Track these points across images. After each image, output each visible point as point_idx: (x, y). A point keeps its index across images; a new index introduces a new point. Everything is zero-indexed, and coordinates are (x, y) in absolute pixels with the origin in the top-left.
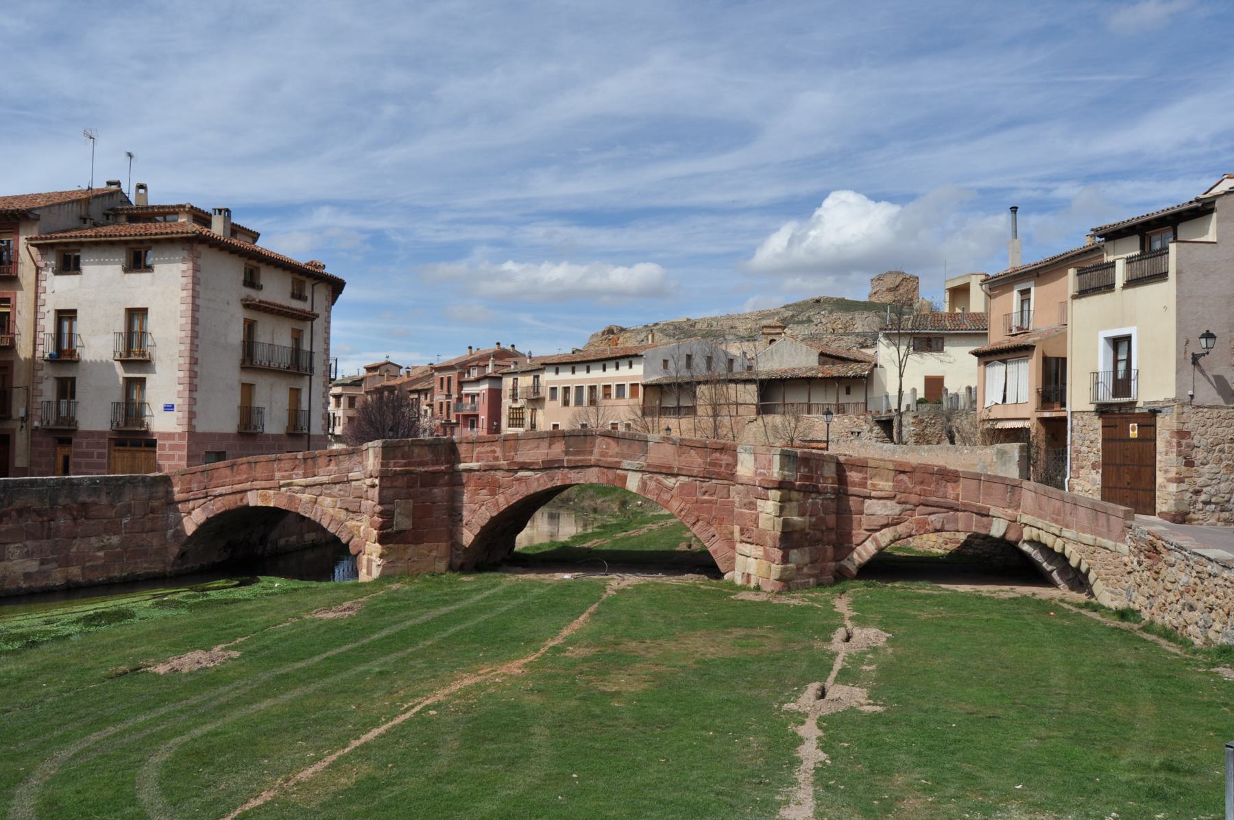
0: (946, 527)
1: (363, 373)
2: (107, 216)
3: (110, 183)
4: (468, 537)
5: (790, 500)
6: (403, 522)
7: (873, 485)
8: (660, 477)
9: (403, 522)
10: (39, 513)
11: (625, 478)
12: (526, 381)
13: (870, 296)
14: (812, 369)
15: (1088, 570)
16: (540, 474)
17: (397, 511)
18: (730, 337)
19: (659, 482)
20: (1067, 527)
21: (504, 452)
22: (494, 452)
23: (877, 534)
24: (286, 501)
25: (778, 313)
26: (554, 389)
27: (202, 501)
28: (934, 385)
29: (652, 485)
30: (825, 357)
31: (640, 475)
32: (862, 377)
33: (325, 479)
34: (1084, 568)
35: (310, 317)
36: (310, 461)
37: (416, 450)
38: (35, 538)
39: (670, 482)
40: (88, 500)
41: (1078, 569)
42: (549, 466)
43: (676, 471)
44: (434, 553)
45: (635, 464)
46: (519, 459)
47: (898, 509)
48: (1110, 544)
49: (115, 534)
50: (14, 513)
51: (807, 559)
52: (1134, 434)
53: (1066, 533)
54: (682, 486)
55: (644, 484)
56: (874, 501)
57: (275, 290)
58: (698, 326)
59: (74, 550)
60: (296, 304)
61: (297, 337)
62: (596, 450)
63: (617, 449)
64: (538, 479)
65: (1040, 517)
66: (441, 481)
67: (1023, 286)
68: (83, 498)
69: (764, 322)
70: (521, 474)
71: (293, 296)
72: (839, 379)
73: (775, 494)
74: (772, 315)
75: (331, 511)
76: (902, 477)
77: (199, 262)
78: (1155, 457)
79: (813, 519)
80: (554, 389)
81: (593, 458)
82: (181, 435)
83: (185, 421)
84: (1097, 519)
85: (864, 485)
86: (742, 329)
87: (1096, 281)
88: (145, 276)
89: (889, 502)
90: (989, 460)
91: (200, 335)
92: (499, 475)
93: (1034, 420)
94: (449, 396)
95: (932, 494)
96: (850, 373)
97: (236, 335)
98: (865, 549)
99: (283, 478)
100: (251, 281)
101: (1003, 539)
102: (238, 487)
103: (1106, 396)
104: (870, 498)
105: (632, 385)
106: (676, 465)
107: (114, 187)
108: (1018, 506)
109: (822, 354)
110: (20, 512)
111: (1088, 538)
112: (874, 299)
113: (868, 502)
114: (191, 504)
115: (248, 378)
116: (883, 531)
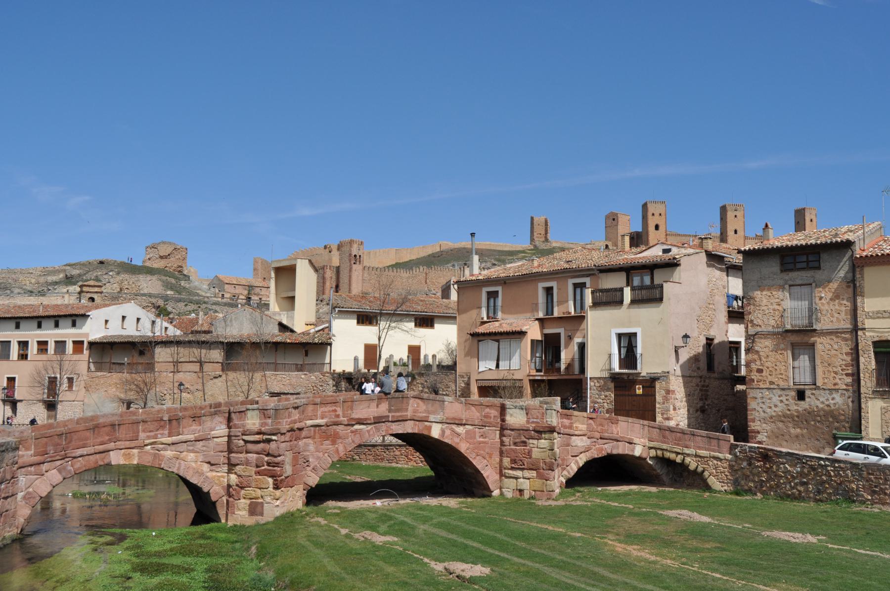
8: (454, 427)
11: (430, 428)
13: (144, 262)
15: (703, 471)
16: (370, 427)
18: (17, 291)
19: (453, 431)
21: (343, 411)
22: (335, 411)
24: (150, 458)
27: (59, 463)
28: (414, 351)
29: (448, 432)
31: (440, 426)
33: (191, 437)
36: (174, 423)
39: (460, 430)
43: (464, 422)
45: (439, 417)
46: (357, 417)
47: (589, 442)
48: (720, 455)
52: (639, 391)
53: (687, 451)
54: (467, 432)
55: (443, 431)
62: (410, 408)
63: (424, 407)
64: (368, 431)
65: (665, 442)
69: (50, 279)
70: (357, 427)
74: (55, 272)
75: (193, 464)
76: (591, 421)
78: (655, 406)
81: (409, 414)
85: (571, 427)
86: (29, 282)
87: (609, 299)
89: (585, 438)
92: (341, 427)
99: (149, 437)
101: (640, 458)
102: (101, 448)
103: (616, 368)
106: (463, 417)
112: (148, 264)
113: (574, 438)
114: (44, 467)
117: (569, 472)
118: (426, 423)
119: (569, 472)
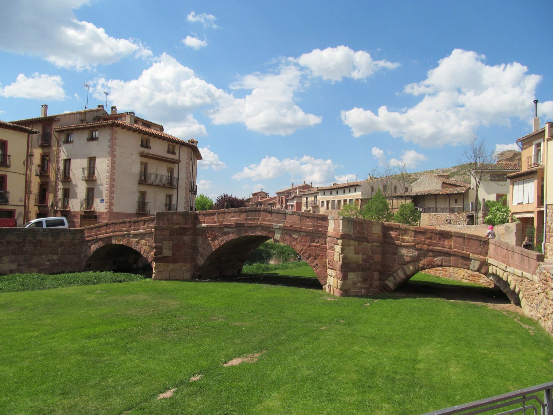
0: (444, 264)
1: (251, 196)
2: (95, 119)
3: (99, 106)
4: (201, 261)
5: (349, 245)
6: (167, 252)
7: (403, 239)
9: (167, 252)
10: (17, 243)
12: (311, 199)
14: (438, 190)
20: (509, 266)
25: (449, 170)
26: (323, 202)
30: (445, 184)
32: (461, 194)
34: (517, 290)
40: (41, 238)
41: (514, 291)
44: (184, 268)
47: (416, 253)
49: (55, 254)
50: (5, 243)
57: (158, 148)
58: (412, 177)
59: (34, 261)
60: (170, 156)
61: (171, 171)
66: (188, 233)
67: (537, 142)
68: (39, 238)
71: (168, 152)
72: (449, 195)
73: (340, 242)
80: (323, 202)
82: (106, 213)
83: (108, 207)
84: (523, 260)
88: (95, 143)
90: (501, 232)
91: (116, 168)
93: (536, 213)
94: (282, 206)
95: (436, 245)
96: (456, 192)
97: (136, 169)
100: (145, 144)
105: (350, 200)
107: (101, 108)
108: (487, 253)
109: (444, 183)
110: (8, 242)
111: (518, 272)
115: (143, 188)
117: (395, 278)
119: (395, 278)
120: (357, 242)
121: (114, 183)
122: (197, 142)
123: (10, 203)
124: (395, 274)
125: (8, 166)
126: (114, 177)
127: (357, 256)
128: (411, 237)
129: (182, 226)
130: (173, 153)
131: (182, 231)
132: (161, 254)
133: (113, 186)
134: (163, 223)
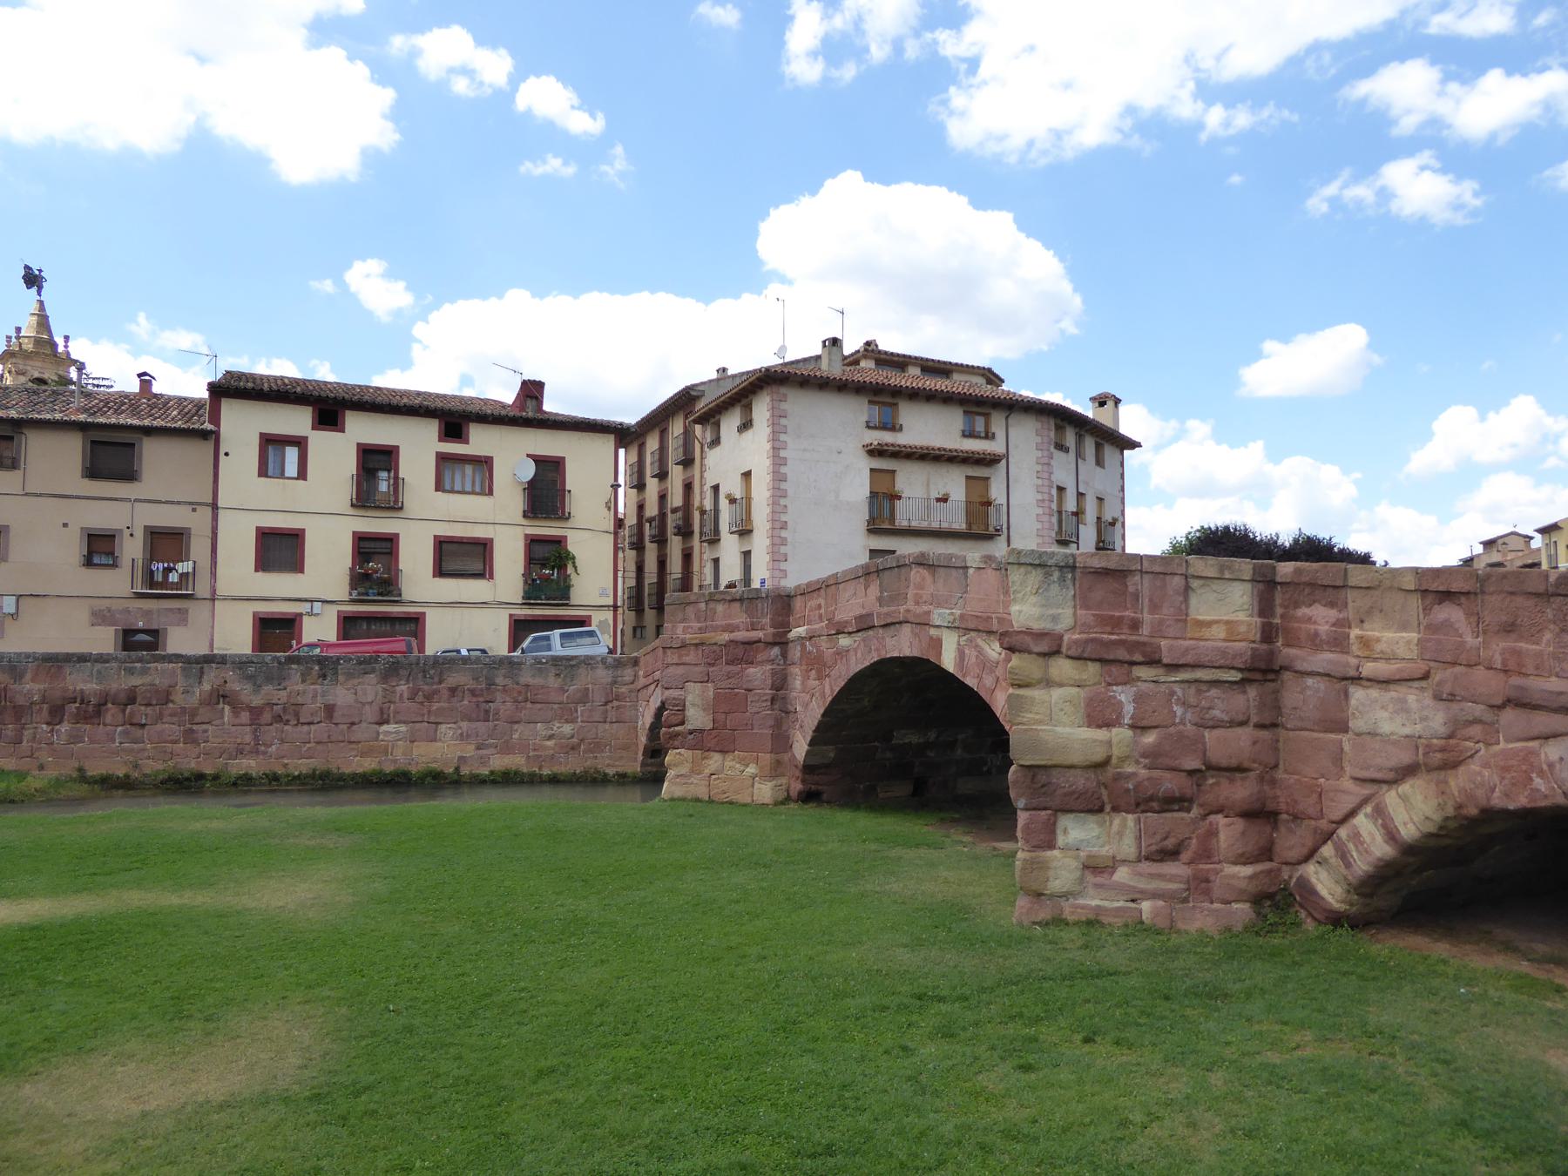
1: (1479, 549)
7: (1365, 642)
10: (473, 692)
11: (937, 644)
17: (690, 698)
19: (980, 652)
23: (1391, 798)
29: (971, 654)
35: (990, 461)
37: (720, 608)
38: (470, 720)
40: (531, 681)
42: (864, 625)
49: (567, 721)
51: (1128, 847)
56: (1374, 693)
62: (911, 593)
66: (760, 657)
71: (969, 434)
77: (784, 406)
79: (1150, 738)
85: (1339, 642)
91: (790, 492)
97: (858, 488)
98: (1356, 836)
104: (1357, 679)
110: (453, 691)
113: (1358, 695)
116: (1405, 788)
117: (1343, 855)
118: (933, 632)
119: (1343, 855)
120: (1093, 668)
121: (784, 534)
122: (1117, 401)
123: (573, 602)
124: (1343, 832)
125: (565, 517)
126: (784, 518)
127: (1101, 734)
128: (1404, 627)
129: (741, 635)
130: (989, 436)
131: (744, 652)
132: (682, 723)
133: (784, 542)
134: (685, 630)
